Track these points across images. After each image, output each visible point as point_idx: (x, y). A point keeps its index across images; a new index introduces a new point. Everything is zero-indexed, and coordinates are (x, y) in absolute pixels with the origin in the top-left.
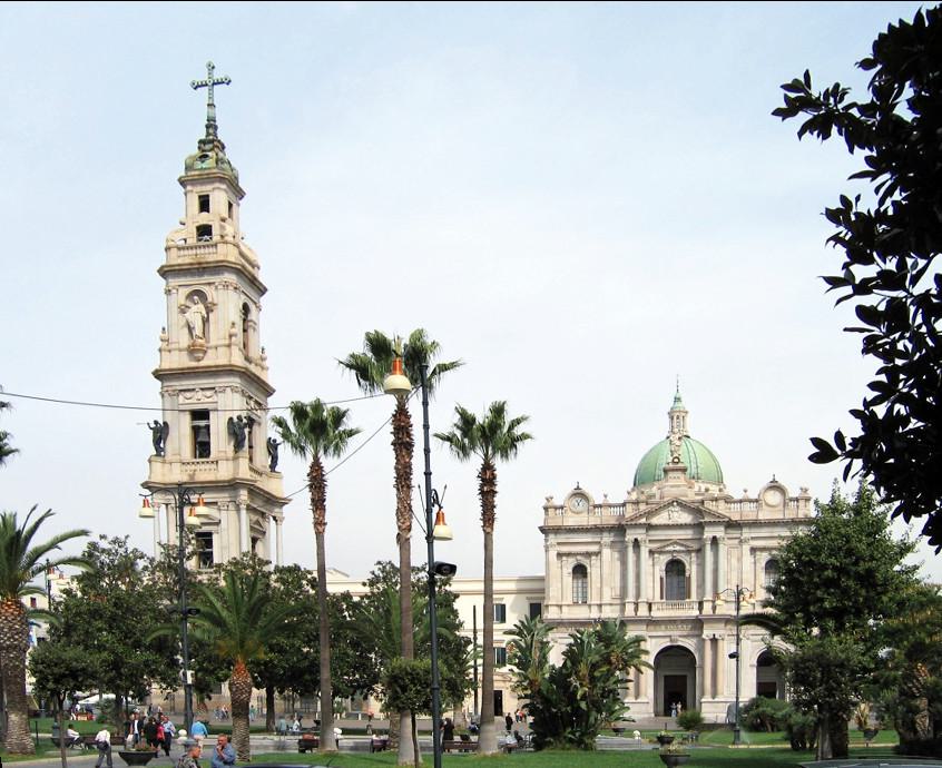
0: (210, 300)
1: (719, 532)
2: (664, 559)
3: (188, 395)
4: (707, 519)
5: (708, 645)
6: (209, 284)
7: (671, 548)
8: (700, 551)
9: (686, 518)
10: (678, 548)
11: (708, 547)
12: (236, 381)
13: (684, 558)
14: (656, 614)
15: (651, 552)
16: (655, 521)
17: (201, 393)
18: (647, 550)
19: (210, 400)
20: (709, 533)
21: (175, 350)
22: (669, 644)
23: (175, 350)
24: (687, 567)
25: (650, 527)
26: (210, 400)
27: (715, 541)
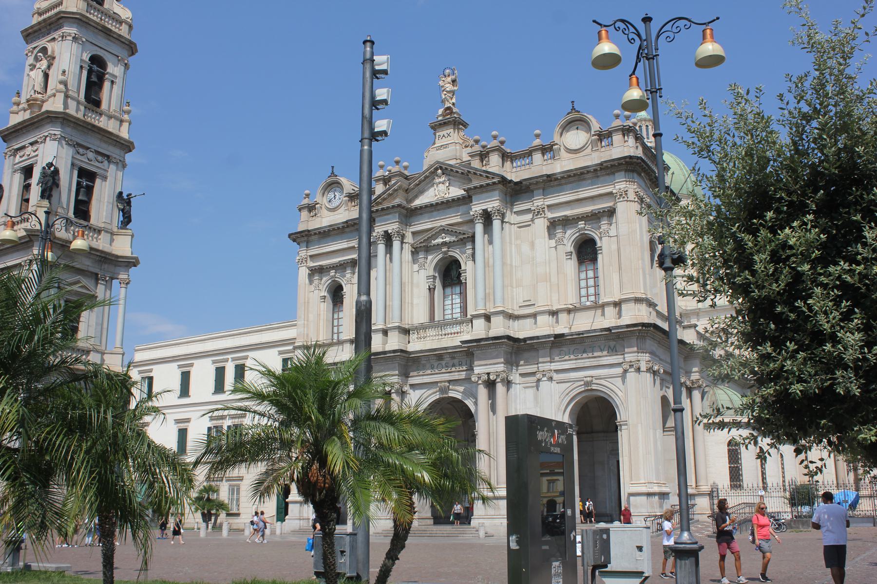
0: (49, 53)
1: (492, 203)
2: (433, 259)
3: (22, 153)
4: (476, 183)
5: (482, 392)
6: (54, 39)
7: (439, 240)
8: (473, 238)
9: (456, 192)
10: (447, 239)
11: (479, 228)
12: (57, 131)
13: (456, 253)
14: (416, 345)
15: (415, 252)
16: (418, 202)
17: (30, 148)
18: (407, 248)
19: (36, 153)
20: (477, 207)
21: (21, 110)
22: (437, 396)
23: (21, 110)
24: (463, 267)
25: (409, 214)
26: (36, 153)
27: (487, 218)
